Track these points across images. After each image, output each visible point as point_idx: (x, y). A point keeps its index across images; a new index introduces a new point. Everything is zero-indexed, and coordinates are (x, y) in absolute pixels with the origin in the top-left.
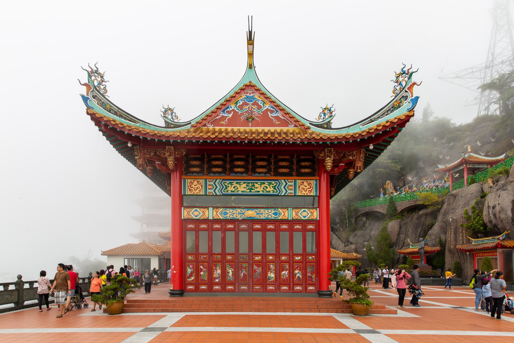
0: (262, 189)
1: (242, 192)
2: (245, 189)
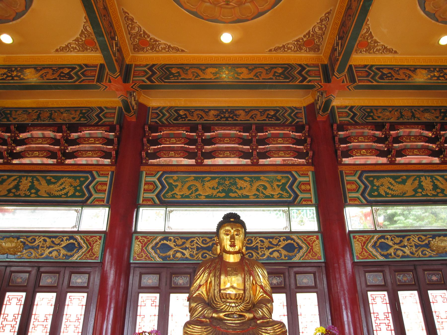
1: (207, 197)
2: (215, 192)
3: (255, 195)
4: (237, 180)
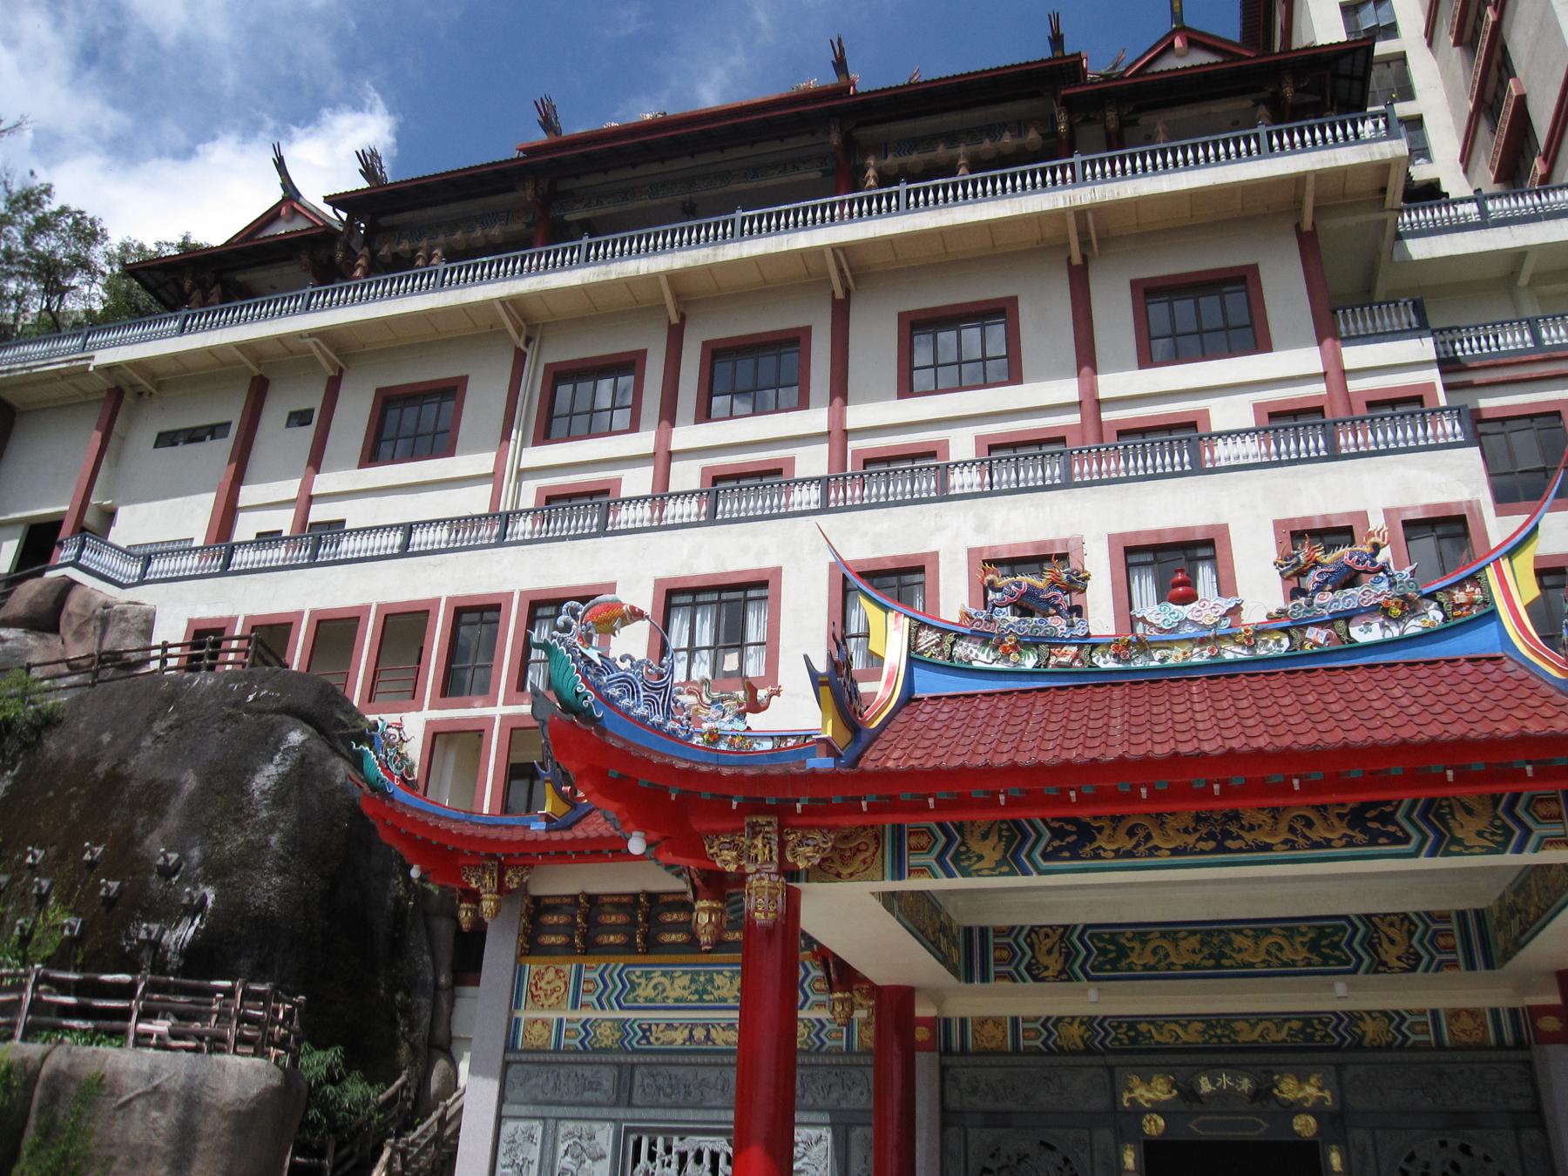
1: (1186, 967)
2: (1197, 958)
3: (1264, 961)
4: (1233, 935)
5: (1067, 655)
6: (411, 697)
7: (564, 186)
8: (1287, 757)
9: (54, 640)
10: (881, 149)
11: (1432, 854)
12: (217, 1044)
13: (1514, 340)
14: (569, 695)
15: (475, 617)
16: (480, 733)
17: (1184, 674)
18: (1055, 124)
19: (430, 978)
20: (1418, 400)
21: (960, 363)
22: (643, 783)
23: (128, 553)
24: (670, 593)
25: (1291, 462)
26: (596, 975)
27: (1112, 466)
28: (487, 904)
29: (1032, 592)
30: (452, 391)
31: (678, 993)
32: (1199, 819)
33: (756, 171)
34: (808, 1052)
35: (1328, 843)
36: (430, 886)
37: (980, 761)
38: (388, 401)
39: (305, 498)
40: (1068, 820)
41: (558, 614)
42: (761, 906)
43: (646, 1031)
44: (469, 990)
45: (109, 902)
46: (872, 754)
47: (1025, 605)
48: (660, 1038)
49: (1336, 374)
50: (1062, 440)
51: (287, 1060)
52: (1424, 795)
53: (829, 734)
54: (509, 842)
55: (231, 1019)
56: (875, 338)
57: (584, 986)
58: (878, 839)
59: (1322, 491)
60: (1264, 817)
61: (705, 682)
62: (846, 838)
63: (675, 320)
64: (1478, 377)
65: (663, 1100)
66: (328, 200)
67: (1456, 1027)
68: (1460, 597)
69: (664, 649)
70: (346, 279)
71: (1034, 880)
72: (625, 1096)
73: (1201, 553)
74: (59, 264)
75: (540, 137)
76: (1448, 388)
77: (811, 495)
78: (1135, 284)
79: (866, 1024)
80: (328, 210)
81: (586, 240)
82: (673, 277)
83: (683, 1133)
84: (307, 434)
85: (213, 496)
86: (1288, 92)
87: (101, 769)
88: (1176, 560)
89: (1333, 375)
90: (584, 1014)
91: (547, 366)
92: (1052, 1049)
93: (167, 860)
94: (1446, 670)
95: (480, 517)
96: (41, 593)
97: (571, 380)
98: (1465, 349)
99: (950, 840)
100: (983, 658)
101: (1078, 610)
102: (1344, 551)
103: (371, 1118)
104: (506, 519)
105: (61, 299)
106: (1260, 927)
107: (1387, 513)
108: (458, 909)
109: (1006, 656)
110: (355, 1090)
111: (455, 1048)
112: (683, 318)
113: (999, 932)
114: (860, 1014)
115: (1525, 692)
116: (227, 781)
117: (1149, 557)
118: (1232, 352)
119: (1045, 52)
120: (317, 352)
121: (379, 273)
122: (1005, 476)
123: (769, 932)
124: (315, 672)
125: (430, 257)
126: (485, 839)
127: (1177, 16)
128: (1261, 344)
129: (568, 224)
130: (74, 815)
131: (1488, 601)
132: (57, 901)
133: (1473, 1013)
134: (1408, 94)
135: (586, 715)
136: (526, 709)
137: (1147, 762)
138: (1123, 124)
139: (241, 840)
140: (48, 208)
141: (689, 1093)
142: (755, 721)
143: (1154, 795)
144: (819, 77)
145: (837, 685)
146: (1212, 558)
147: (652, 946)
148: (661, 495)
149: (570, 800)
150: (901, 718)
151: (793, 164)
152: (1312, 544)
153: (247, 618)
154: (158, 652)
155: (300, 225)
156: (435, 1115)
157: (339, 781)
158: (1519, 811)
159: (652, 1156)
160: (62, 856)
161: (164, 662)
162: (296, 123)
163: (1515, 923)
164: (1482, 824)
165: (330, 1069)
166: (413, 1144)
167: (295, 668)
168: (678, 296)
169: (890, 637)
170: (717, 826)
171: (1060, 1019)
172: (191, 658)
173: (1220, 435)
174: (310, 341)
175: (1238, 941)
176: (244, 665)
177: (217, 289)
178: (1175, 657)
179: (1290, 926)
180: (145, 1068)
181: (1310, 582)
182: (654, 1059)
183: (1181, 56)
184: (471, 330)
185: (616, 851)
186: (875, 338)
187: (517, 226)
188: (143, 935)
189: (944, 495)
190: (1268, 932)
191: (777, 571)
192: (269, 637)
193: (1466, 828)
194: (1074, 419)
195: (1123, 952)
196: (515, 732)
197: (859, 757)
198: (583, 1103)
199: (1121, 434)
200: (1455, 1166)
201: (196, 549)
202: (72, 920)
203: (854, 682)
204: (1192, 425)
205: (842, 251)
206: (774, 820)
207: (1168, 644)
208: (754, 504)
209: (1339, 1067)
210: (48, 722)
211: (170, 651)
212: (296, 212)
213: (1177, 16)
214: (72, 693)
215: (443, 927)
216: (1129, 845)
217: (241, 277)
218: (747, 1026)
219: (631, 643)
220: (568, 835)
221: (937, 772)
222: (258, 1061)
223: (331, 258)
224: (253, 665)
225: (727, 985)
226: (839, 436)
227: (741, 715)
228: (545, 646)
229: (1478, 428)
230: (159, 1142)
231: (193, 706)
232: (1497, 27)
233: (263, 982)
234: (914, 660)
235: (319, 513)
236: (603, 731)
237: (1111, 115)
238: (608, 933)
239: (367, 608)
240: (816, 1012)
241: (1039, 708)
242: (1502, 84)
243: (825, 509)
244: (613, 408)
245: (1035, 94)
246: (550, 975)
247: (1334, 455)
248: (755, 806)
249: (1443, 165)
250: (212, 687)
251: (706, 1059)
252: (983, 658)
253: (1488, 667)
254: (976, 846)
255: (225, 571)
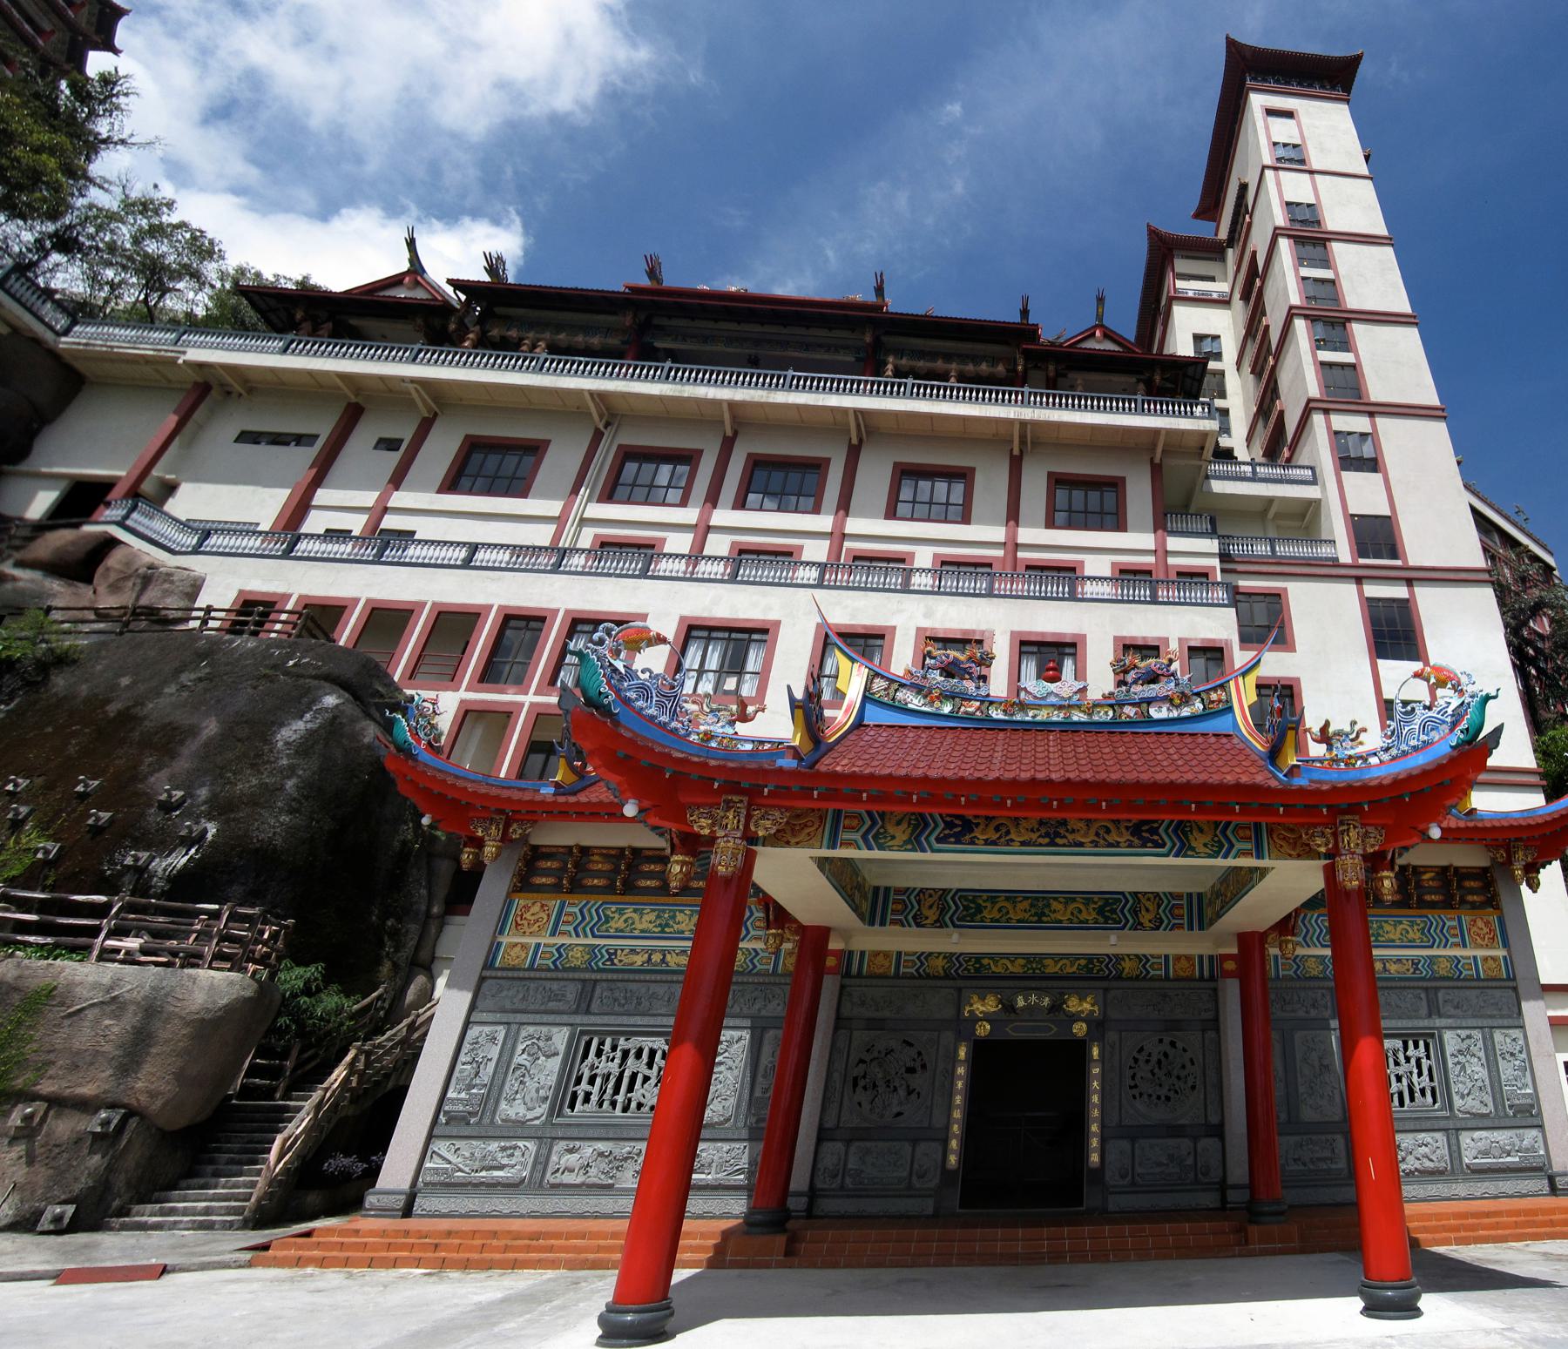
0: (1068, 916)
1: (1019, 921)
5: (972, 707)
6: (451, 679)
7: (656, 321)
8: (1102, 786)
9: (85, 591)
10: (899, 353)
11: (1177, 855)
12: (192, 959)
13: (1262, 549)
14: (593, 693)
15: (522, 624)
16: (509, 714)
17: (1046, 727)
18: (1016, 364)
19: (423, 908)
20: (1206, 575)
21: (931, 503)
22: (644, 763)
23: (187, 526)
24: (691, 628)
25: (1129, 602)
26: (576, 910)
27: (1019, 587)
28: (489, 850)
29: (956, 662)
30: (536, 449)
31: (645, 926)
32: (1041, 823)
33: (807, 347)
34: (741, 973)
35: (1117, 845)
36: (439, 833)
37: (903, 772)
38: (473, 447)
39: (380, 508)
40: (957, 817)
41: (595, 631)
42: (723, 861)
43: (612, 954)
44: (458, 919)
45: (97, 830)
46: (827, 760)
47: (949, 671)
48: (622, 960)
49: (1162, 552)
50: (990, 565)
51: (265, 975)
52: (1177, 817)
53: (797, 743)
54: (519, 801)
55: (211, 938)
56: (874, 476)
57: (564, 918)
58: (822, 819)
59: (1146, 622)
60: (1082, 824)
61: (707, 695)
62: (798, 816)
63: (729, 433)
64: (1240, 568)
65: (617, 1008)
66: (450, 282)
67: (1179, 966)
68: (1214, 696)
69: (679, 667)
70: (453, 344)
71: (928, 856)
72: (584, 1006)
73: (1068, 650)
74: (166, 268)
75: (645, 282)
76: (1223, 571)
77: (813, 574)
78: (1050, 474)
79: (790, 953)
80: (449, 290)
81: (668, 364)
82: (732, 405)
83: (629, 1035)
84: (394, 458)
85: (288, 492)
86: (1157, 378)
87: (113, 709)
88: (1051, 653)
89: (1160, 553)
90: (559, 940)
91: (620, 446)
92: (924, 976)
93: (170, 796)
94: (1201, 740)
95: (540, 548)
96: (73, 543)
97: (635, 459)
98: (1235, 550)
99: (874, 823)
100: (915, 702)
101: (984, 678)
102: (1152, 661)
103: (342, 1024)
104: (563, 553)
105: (160, 298)
106: (1069, 896)
107: (1180, 640)
108: (462, 852)
109: (931, 703)
110: (331, 1000)
111: (436, 967)
112: (736, 433)
113: (899, 891)
114: (787, 946)
115: (1241, 757)
116: (251, 734)
117: (1035, 649)
118: (1102, 528)
119: (1016, 318)
120: (415, 395)
121: (486, 347)
122: (949, 583)
123: (727, 881)
124: (361, 649)
125: (533, 347)
126: (497, 798)
127: (1100, 317)
128: (1121, 526)
129: (657, 349)
130: (72, 750)
131: (1229, 701)
132: (33, 828)
133: (1188, 958)
134: (1223, 395)
135: (605, 710)
136: (554, 700)
137: (1014, 783)
138: (1058, 375)
139: (254, 781)
140: (165, 219)
141: (639, 1004)
142: (742, 729)
143: (1015, 806)
144: (864, 295)
145: (808, 709)
146: (1074, 655)
147: (629, 888)
148: (696, 555)
149: (580, 773)
150: (852, 737)
151: (837, 348)
152: (1137, 654)
153: (301, 597)
154: (201, 614)
155: (420, 294)
156: (406, 1022)
157: (366, 740)
158: (1229, 833)
159: (599, 1053)
160: (49, 787)
161: (205, 622)
162: (439, 218)
163: (1218, 902)
164: (1207, 839)
165: (307, 983)
166: (380, 1046)
167: (341, 643)
168: (734, 418)
169: (853, 680)
170: (699, 800)
171: (930, 954)
172: (235, 623)
173: (1089, 578)
174: (411, 386)
175: (1055, 905)
176: (290, 635)
177: (330, 325)
178: (1042, 715)
179: (1087, 897)
180: (106, 980)
181: (1130, 677)
182: (615, 976)
183: (1099, 342)
184: (564, 408)
185: (613, 814)
186: (874, 476)
187: (614, 341)
188: (129, 861)
189: (906, 589)
190: (1074, 900)
191: (777, 623)
192: (321, 616)
193: (1198, 840)
194: (1000, 553)
195: (979, 909)
196: (540, 717)
197: (817, 762)
198: (547, 1012)
199: (1028, 567)
200: (1166, 1055)
201: (260, 533)
202: (49, 845)
203: (821, 709)
204: (1073, 569)
205: (860, 413)
206: (745, 799)
207: (1039, 707)
208: (768, 573)
209: (1106, 990)
210: (62, 660)
211: (213, 614)
212: (418, 284)
213: (1100, 317)
214: (94, 638)
215: (444, 868)
216: (995, 837)
217: (354, 322)
218: (696, 953)
219: (653, 660)
220: (572, 799)
221: (872, 777)
222: (233, 975)
223: (445, 327)
224: (299, 636)
225: (686, 921)
226: (838, 537)
227: (732, 723)
228: (579, 654)
229: (1237, 597)
230: (107, 1048)
231: (227, 664)
232: (1274, 368)
233: (252, 906)
234: (867, 698)
235: (390, 522)
236: (617, 723)
237: (1051, 367)
238: (594, 877)
239: (423, 604)
240: (754, 943)
241: (949, 740)
242: (1273, 401)
243: (820, 585)
244: (669, 487)
245: (1006, 343)
246: (536, 908)
247: (1154, 601)
248: (733, 787)
249: (1236, 441)
250: (252, 650)
251: (659, 977)
252: (915, 702)
253: (1224, 740)
254: (891, 830)
255: (287, 554)
